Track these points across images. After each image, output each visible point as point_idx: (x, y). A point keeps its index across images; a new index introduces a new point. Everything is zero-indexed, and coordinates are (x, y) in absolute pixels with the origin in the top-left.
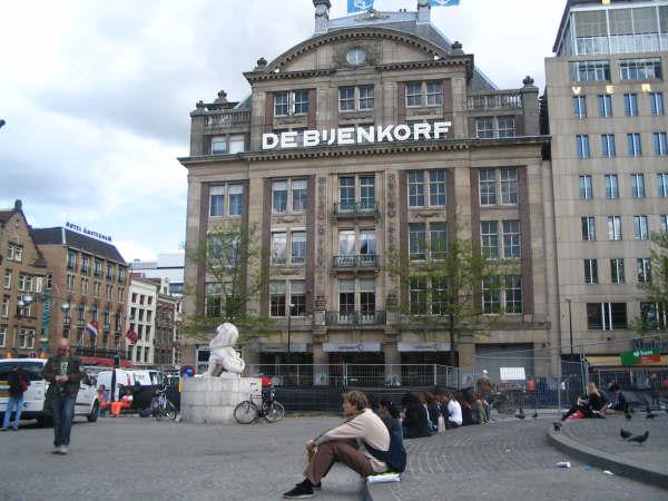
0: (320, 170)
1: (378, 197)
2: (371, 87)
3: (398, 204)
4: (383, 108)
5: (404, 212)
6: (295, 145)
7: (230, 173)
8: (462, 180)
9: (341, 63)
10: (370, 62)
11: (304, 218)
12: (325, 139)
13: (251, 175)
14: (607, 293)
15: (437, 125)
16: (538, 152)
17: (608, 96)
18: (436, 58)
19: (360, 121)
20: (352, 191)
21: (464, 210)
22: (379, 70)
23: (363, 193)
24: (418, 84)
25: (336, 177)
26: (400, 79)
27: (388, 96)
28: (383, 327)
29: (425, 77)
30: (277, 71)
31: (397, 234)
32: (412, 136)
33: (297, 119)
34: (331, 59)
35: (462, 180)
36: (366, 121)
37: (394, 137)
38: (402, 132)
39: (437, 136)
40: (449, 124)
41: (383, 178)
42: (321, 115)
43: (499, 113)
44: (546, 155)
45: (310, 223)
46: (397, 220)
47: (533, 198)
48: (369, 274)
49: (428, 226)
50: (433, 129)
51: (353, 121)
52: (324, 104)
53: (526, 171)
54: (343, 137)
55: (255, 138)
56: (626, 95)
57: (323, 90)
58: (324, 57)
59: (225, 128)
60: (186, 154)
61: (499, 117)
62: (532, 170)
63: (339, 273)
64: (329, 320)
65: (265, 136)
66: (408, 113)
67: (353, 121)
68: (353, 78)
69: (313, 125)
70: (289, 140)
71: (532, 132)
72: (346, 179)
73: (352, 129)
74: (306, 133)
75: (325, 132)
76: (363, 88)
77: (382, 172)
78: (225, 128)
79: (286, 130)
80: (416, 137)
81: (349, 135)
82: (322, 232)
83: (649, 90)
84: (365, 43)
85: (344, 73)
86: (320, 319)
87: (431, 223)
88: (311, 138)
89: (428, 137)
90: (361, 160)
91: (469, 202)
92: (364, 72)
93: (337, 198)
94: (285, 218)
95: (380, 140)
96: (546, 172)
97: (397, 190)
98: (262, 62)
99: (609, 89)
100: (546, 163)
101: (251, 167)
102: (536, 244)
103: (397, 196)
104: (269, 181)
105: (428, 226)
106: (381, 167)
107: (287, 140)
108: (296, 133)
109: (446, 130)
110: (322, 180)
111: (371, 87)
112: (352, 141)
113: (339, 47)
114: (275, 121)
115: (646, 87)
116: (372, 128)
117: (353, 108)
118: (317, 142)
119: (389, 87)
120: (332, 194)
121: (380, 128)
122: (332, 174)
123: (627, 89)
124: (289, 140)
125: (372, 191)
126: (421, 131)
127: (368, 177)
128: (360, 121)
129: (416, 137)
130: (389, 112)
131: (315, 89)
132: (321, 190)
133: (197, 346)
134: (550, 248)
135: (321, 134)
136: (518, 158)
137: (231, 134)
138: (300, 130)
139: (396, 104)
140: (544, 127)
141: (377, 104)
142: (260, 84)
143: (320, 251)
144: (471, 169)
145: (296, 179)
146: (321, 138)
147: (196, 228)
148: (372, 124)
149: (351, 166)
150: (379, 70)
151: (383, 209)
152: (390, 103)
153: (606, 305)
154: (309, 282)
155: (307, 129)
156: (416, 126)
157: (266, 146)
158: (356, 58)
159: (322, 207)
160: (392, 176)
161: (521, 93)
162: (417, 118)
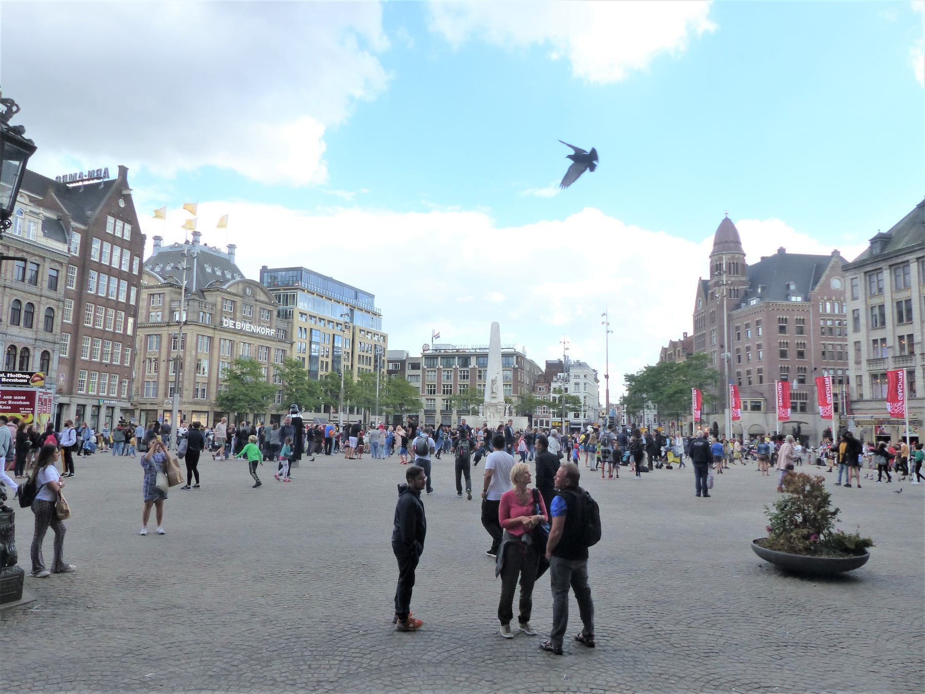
0: (237, 338)
6: (233, 327)
9: (245, 293)
13: (216, 336)
15: (272, 330)
19: (247, 320)
54: (247, 327)
55: (218, 319)
88: (239, 325)
90: (249, 338)
101: (216, 332)
104: (220, 339)
108: (234, 322)
110: (237, 344)
118: (239, 328)
132: (237, 347)
150: (256, 300)
160: (256, 347)
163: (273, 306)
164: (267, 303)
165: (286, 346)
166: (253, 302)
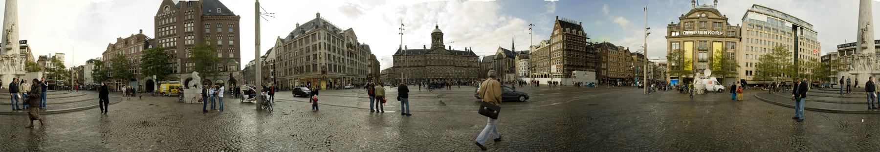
10: (707, 16)
14: (749, 69)
16: (739, 39)
42: (696, 27)
44: (740, 40)
47: (737, 49)
54: (701, 33)
55: (681, 32)
62: (738, 43)
71: (738, 35)
84: (706, 12)
98: (683, 15)
99: (753, 30)
102: (737, 58)
119: (710, 22)
127: (706, 41)
134: (740, 59)
140: (740, 35)
149: (702, 39)
151: (709, 49)
152: (711, 26)
158: (704, 15)
161: (737, 27)
165: (737, 40)
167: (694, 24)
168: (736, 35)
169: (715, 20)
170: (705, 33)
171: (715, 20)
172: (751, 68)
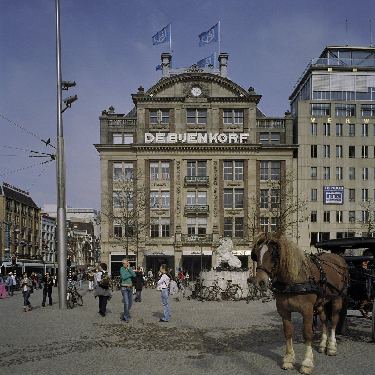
0: (178, 156)
1: (208, 174)
2: (205, 110)
3: (219, 178)
4: (212, 123)
5: (222, 183)
7: (126, 155)
8: (252, 167)
10: (205, 94)
11: (169, 183)
12: (180, 139)
15: (241, 135)
17: (329, 124)
18: (241, 96)
19: (198, 130)
20: (194, 170)
21: (252, 183)
22: (210, 100)
23: (200, 172)
24: (230, 110)
25: (185, 161)
26: (223, 107)
27: (214, 116)
28: (211, 243)
29: (235, 107)
30: (152, 95)
31: (218, 194)
32: (228, 140)
33: (164, 126)
34: (182, 91)
35: (252, 167)
36: (202, 130)
37: (218, 141)
38: (222, 138)
39: (241, 141)
40: (248, 135)
41: (211, 164)
42: (178, 125)
43: (273, 131)
44: (296, 155)
45: (172, 186)
46: (218, 187)
48: (205, 215)
49: (234, 190)
50: (239, 137)
51: (195, 130)
52: (179, 118)
53: (284, 164)
54: (189, 139)
55: (140, 136)
56: (338, 124)
57: (178, 109)
58: (178, 90)
59: (121, 128)
60: (99, 143)
61: (272, 132)
62: (288, 163)
63: (188, 214)
64: (183, 239)
65: (147, 135)
66: (225, 127)
67: (195, 130)
68: (195, 104)
69: (172, 130)
70: (160, 138)
71: (289, 142)
72: (190, 162)
73: (196, 134)
74: (170, 135)
75: (180, 135)
76: (200, 110)
77: (210, 160)
78: (121, 128)
79: (158, 132)
80: (230, 141)
81: (194, 138)
82: (178, 192)
83: (349, 122)
84: (201, 83)
85: (190, 101)
86: (179, 238)
87: (235, 189)
88: (172, 138)
89: (236, 141)
91: (255, 179)
92: (201, 101)
93: (186, 174)
94: (158, 183)
95: (211, 141)
96: (295, 165)
97: (218, 170)
98: (141, 89)
99: (329, 121)
100: (295, 160)
101: (138, 153)
103: (218, 174)
105: (234, 190)
106: (209, 157)
107: (158, 138)
108: (164, 134)
109: (246, 138)
110: (178, 163)
111: (205, 110)
112: (196, 141)
113: (186, 84)
114: (150, 127)
115: (348, 121)
116: (206, 135)
117: (193, 122)
119: (214, 111)
120: (183, 171)
121: (211, 135)
122: (183, 160)
123: (338, 121)
124: (160, 138)
125: (205, 171)
126: (233, 138)
127: (203, 162)
128: (198, 130)
129: (230, 141)
130: (214, 126)
131: (174, 109)
132: (178, 168)
133: (110, 252)
135: (178, 136)
136: (281, 156)
137: (125, 133)
138: (167, 133)
139: (218, 122)
140: (295, 139)
141: (209, 121)
142: (142, 103)
143: (178, 201)
144: (257, 160)
145: (164, 161)
146: (178, 138)
147: (106, 186)
148: (206, 132)
149: (194, 156)
151: (211, 181)
152: (215, 121)
153: (320, 234)
154: (172, 218)
155: (169, 132)
156: (230, 135)
157: (147, 141)
158: (196, 92)
159: (178, 178)
160: (216, 163)
162: (230, 130)
163: (245, 101)
164: (236, 101)
165: (286, 156)
166: (205, 104)
167: (172, 115)
168: (282, 140)
169: (227, 105)
170: (202, 139)
171: (227, 105)
172: (327, 225)
